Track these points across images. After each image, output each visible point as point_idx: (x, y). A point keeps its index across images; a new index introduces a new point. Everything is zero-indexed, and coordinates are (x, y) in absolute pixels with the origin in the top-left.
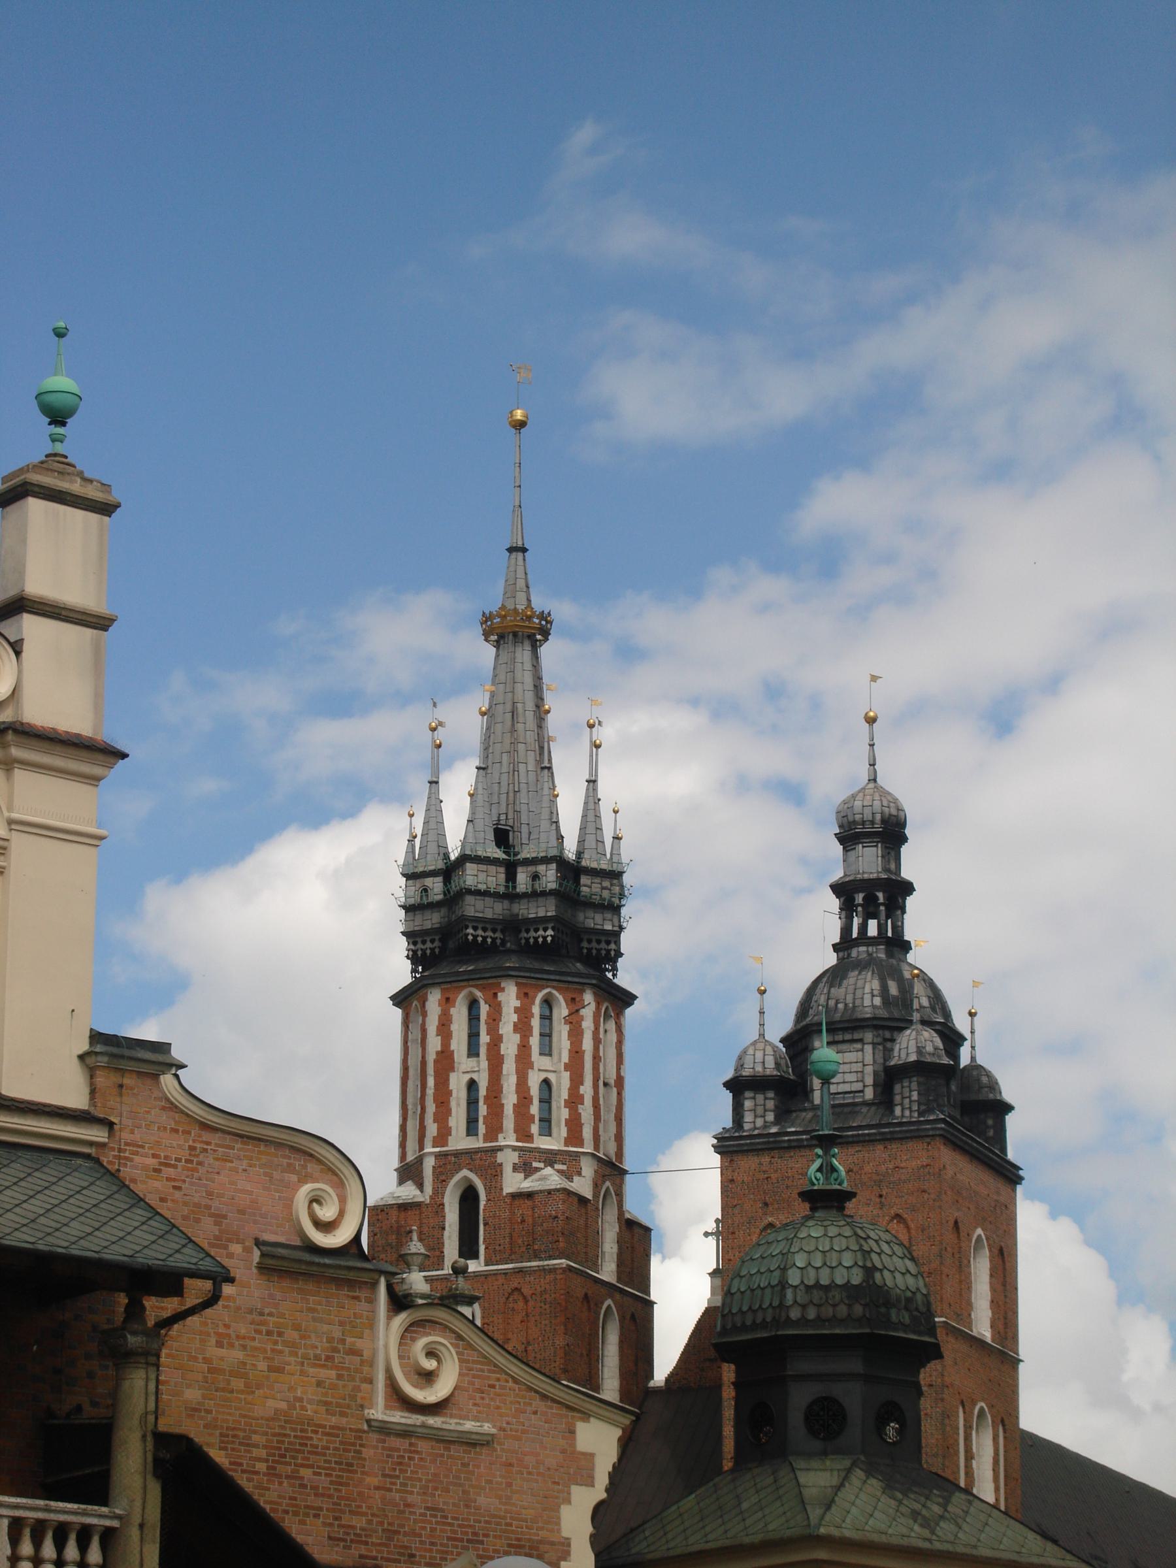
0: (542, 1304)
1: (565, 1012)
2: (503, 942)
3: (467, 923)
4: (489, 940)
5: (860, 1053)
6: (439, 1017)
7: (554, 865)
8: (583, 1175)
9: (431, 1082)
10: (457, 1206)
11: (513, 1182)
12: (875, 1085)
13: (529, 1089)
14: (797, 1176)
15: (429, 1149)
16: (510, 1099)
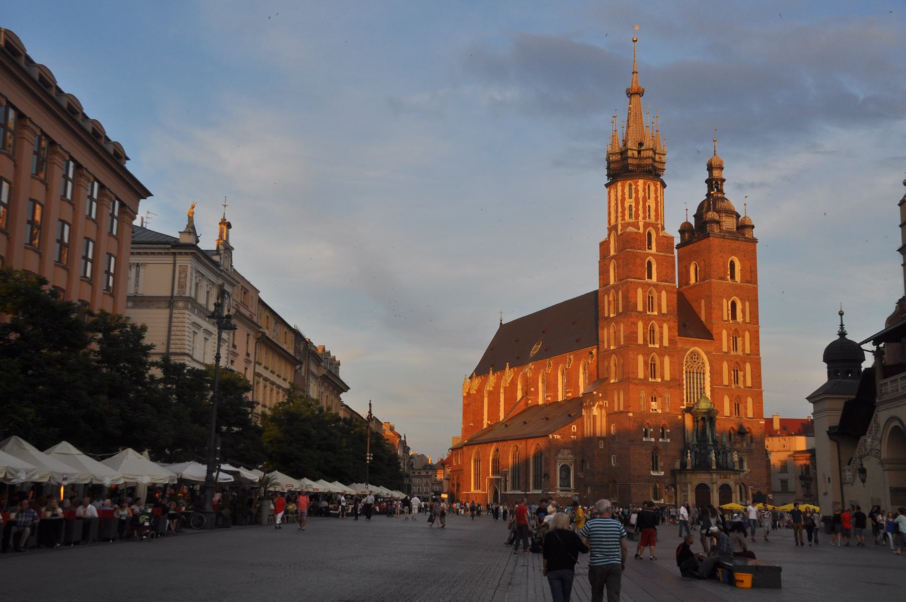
9: (641, 203)
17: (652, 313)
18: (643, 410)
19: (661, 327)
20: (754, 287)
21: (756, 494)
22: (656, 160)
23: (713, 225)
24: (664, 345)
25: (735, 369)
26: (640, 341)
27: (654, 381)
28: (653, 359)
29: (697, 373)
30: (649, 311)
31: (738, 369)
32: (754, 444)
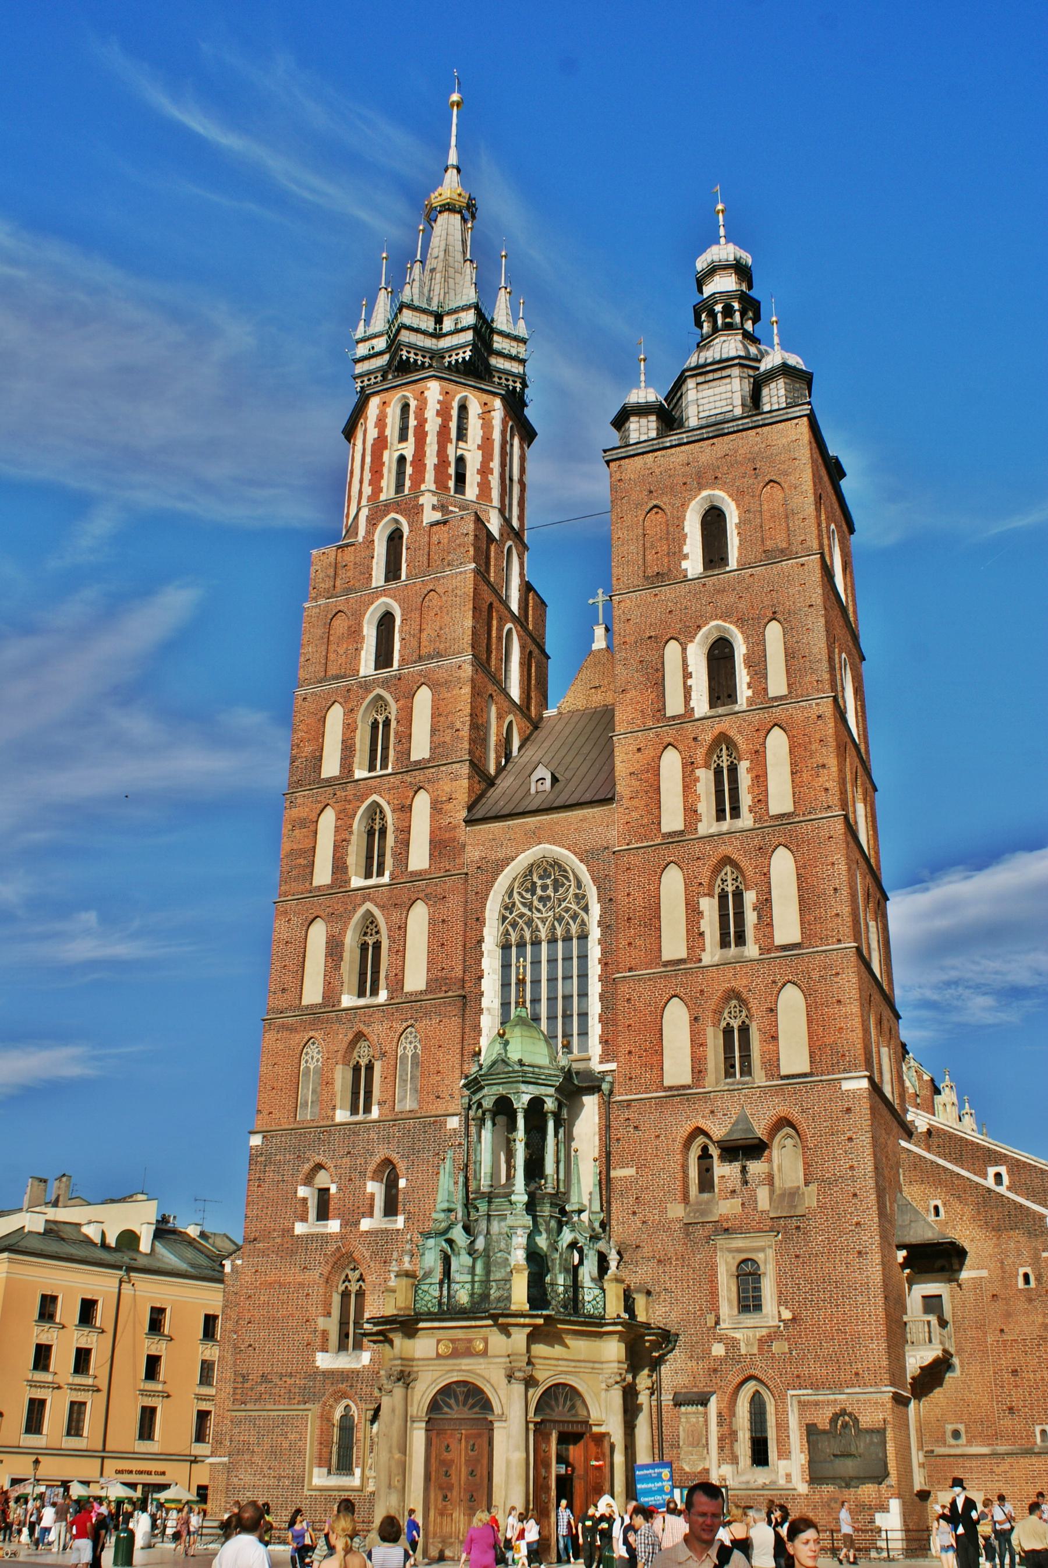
0: (454, 599)
1: (480, 411)
2: (430, 366)
3: (402, 347)
4: (419, 362)
5: (729, 386)
6: (378, 416)
7: (473, 310)
8: (491, 521)
9: (368, 459)
10: (385, 543)
11: (430, 516)
12: (743, 405)
13: (448, 456)
14: (678, 467)
15: (364, 502)
16: (431, 460)
17: (379, 772)
18: (309, 1118)
19: (405, 809)
20: (803, 565)
21: (823, 1423)
22: (444, 331)
23: (627, 425)
24: (410, 869)
25: (730, 889)
26: (323, 875)
27: (362, 1002)
28: (369, 923)
29: (552, 941)
30: (372, 768)
31: (742, 887)
32: (813, 1187)
